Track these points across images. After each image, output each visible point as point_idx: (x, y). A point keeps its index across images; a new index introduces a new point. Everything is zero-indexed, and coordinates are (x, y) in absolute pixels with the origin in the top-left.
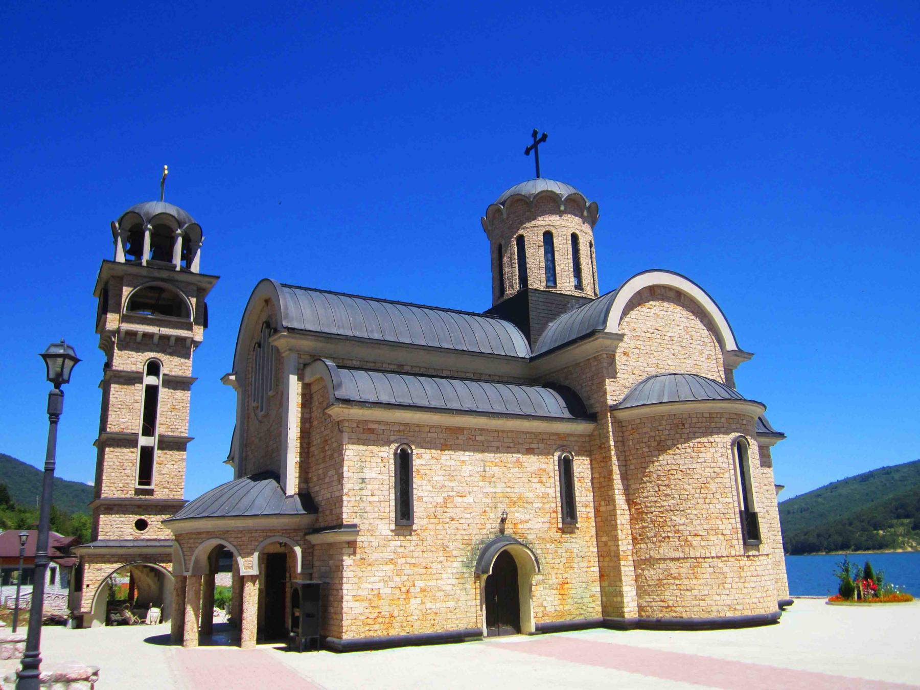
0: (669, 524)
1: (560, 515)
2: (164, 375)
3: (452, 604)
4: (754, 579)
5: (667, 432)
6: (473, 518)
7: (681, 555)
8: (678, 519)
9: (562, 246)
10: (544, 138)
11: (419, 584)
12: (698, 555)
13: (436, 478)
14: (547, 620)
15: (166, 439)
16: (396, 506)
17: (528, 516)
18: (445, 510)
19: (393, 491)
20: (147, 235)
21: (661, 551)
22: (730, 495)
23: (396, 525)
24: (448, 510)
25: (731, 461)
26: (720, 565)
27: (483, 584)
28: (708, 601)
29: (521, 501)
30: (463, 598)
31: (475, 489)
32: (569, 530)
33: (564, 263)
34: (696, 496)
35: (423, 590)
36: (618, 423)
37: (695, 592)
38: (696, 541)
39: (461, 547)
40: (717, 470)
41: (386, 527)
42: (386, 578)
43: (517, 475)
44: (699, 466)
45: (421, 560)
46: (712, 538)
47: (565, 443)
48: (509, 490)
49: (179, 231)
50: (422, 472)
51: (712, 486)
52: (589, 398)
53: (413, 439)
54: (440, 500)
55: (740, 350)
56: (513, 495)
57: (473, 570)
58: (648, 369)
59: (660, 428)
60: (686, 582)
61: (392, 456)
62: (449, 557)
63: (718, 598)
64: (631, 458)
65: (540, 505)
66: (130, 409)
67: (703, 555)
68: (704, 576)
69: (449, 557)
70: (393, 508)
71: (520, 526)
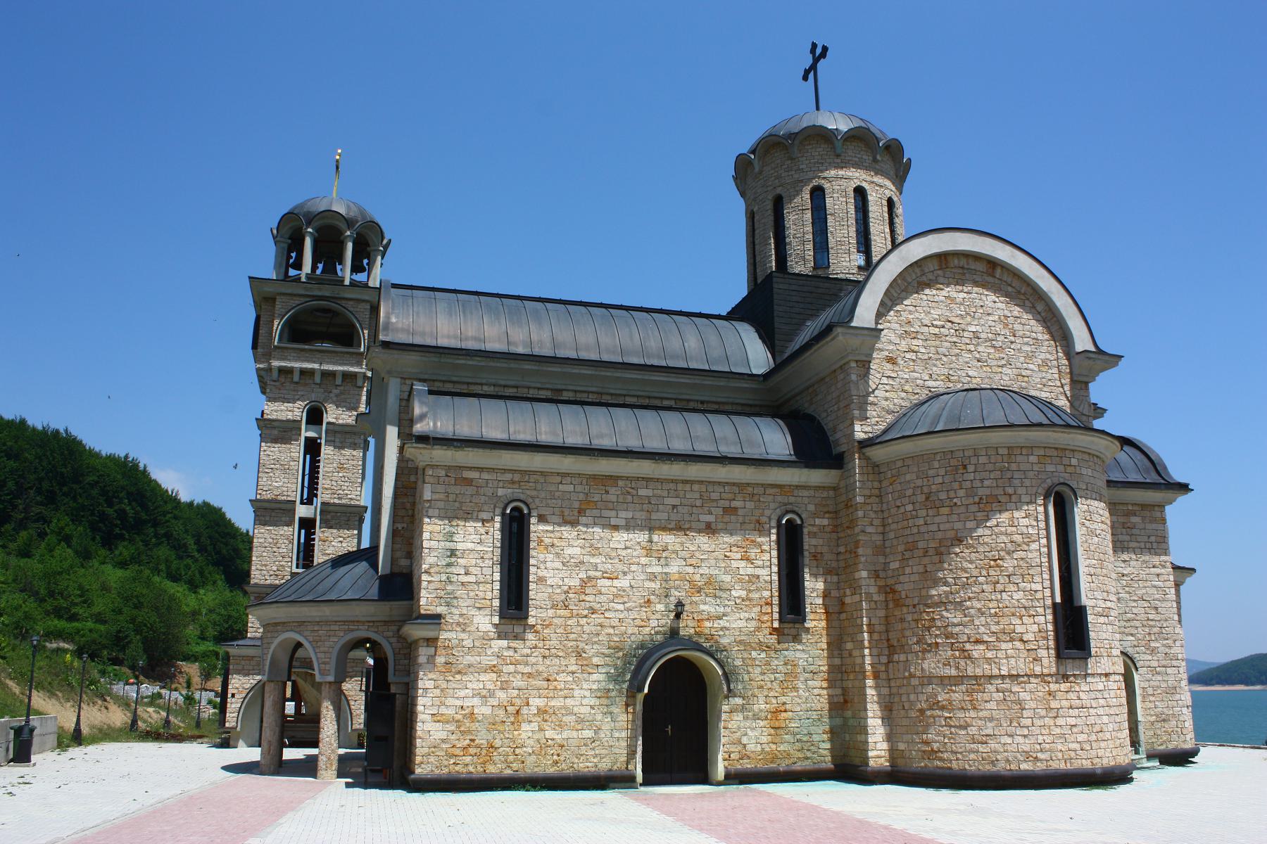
0: (939, 623)
1: (776, 609)
2: (328, 423)
3: (588, 734)
4: (1076, 712)
5: (940, 480)
6: (628, 610)
7: (954, 672)
8: (953, 617)
9: (840, 206)
11: (536, 702)
12: (979, 672)
13: (569, 551)
14: (748, 765)
15: (331, 508)
16: (501, 590)
17: (722, 610)
18: (583, 597)
19: (497, 568)
21: (926, 666)
22: (1037, 579)
23: (501, 617)
24: (587, 598)
25: (1042, 525)
26: (1015, 689)
27: (639, 707)
28: (993, 745)
29: (713, 588)
30: (606, 727)
31: (634, 568)
32: (793, 632)
33: (842, 231)
34: (981, 579)
35: (541, 712)
36: (874, 468)
37: (973, 730)
38: (977, 651)
39: (606, 651)
40: (1018, 538)
41: (485, 622)
42: (484, 692)
43: (705, 547)
44: (988, 532)
45: (541, 668)
46: (1004, 646)
47: (792, 499)
48: (690, 570)
49: (348, 233)
50: (547, 541)
51: (1009, 564)
52: (835, 431)
53: (534, 493)
54: (575, 582)
55: (1100, 351)
56: (697, 577)
57: (625, 686)
58: (931, 383)
59: (931, 472)
60: (960, 714)
63: (1009, 740)
64: (890, 521)
65: (743, 594)
66: (286, 470)
67: (988, 673)
68: (988, 706)
69: (586, 667)
70: (497, 593)
71: (707, 624)
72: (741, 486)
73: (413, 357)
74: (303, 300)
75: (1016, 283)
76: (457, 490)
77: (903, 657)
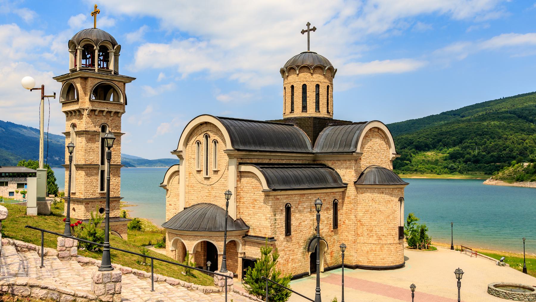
3: (300, 264)
10: (314, 29)
11: (291, 257)
20: (96, 51)
38: (383, 238)
54: (298, 224)
61: (284, 209)
62: (300, 246)
69: (300, 246)
72: (326, 193)
73: (244, 153)
74: (101, 80)
75: (382, 134)
76: (276, 202)
77: (362, 238)
